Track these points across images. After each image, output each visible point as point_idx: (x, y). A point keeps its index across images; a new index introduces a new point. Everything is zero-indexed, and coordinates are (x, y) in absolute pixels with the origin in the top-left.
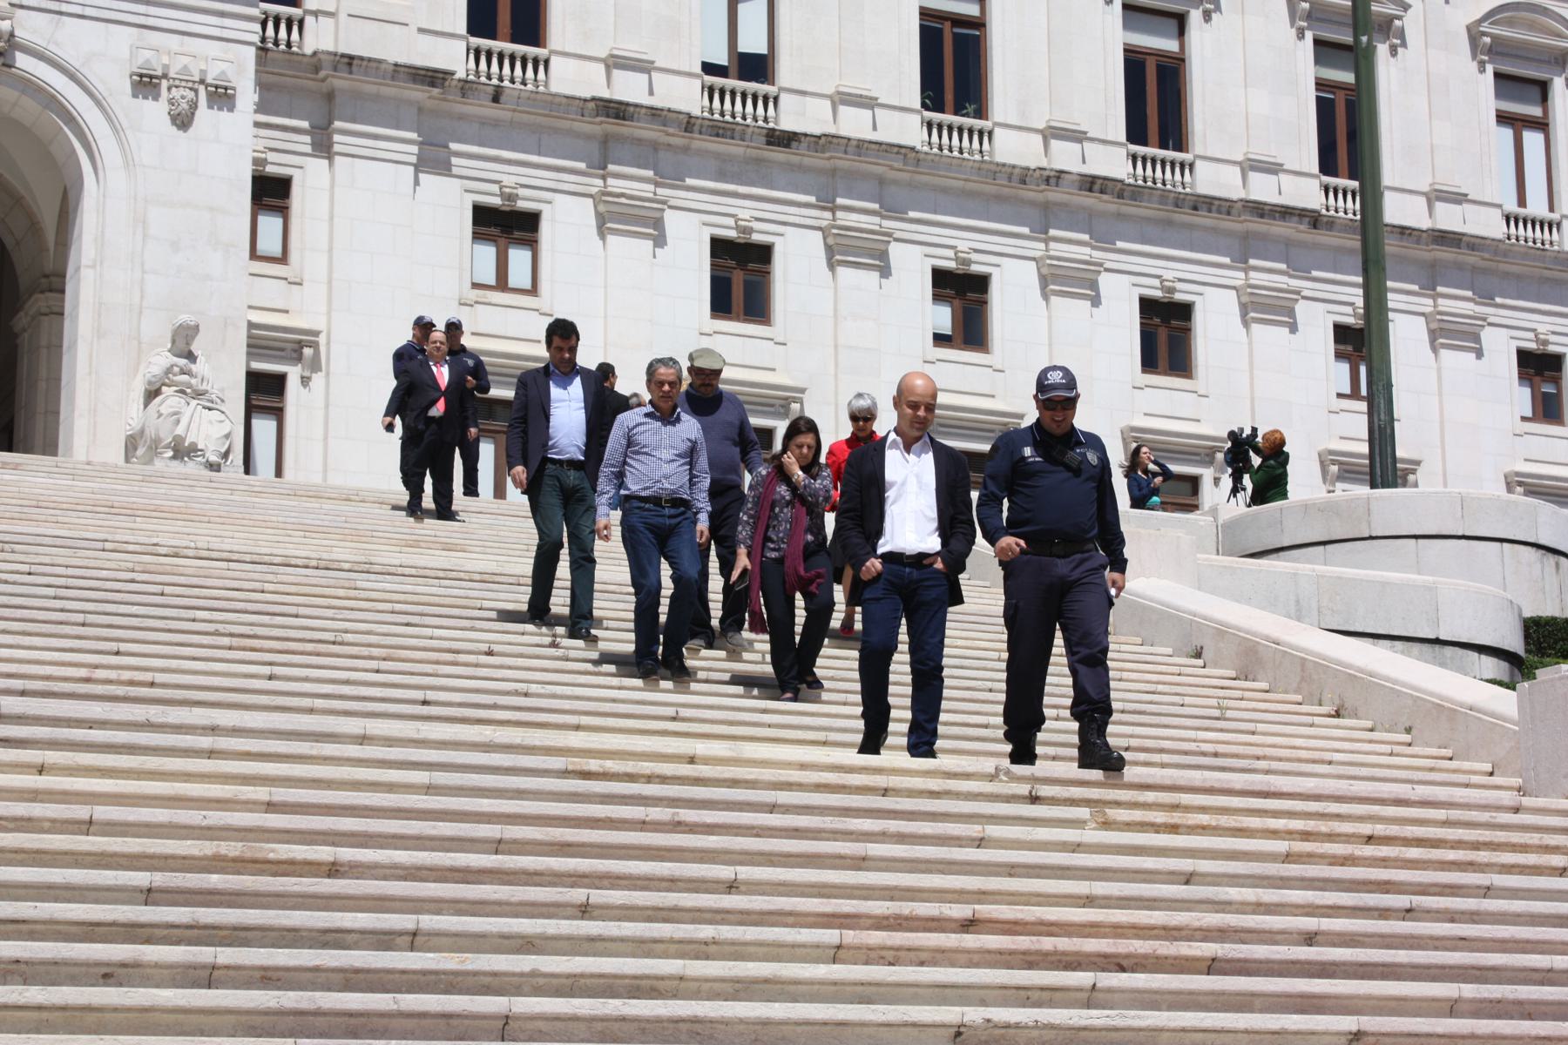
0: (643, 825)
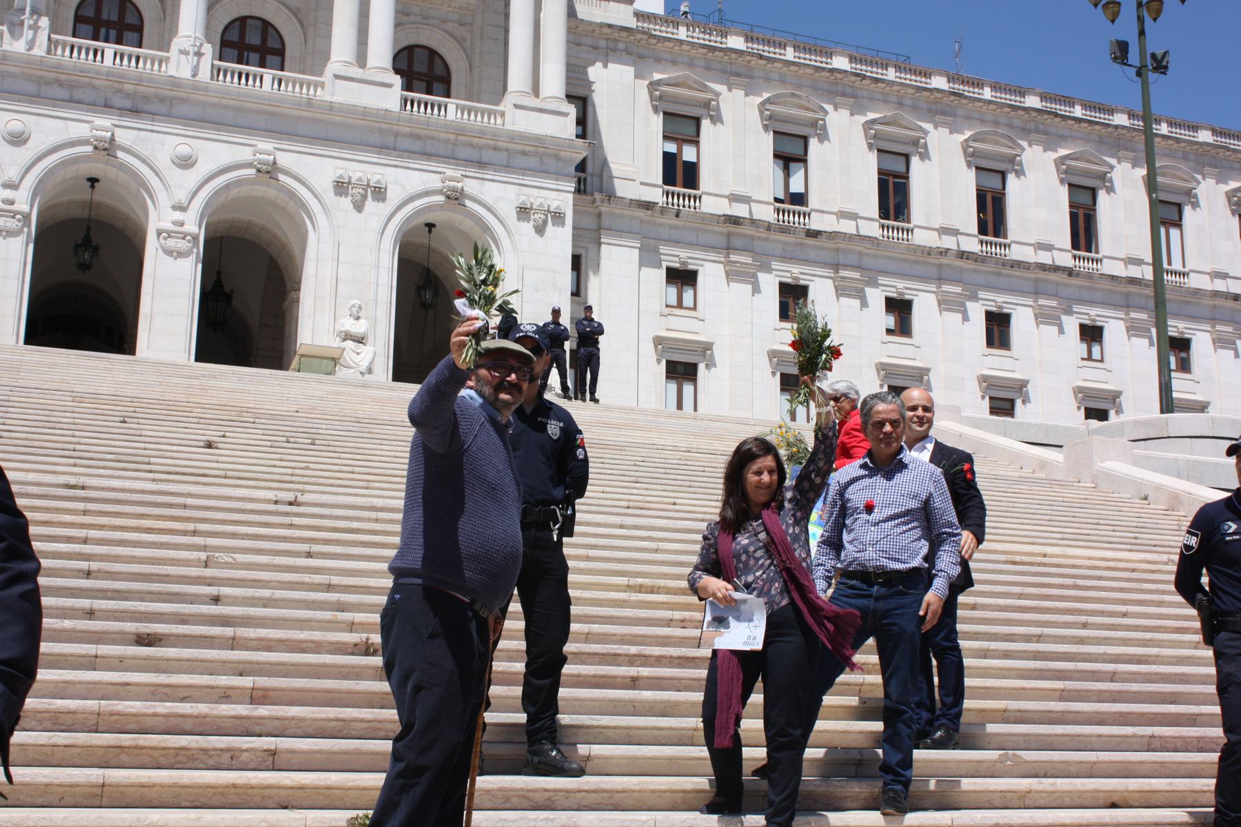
0: (1062, 586)
